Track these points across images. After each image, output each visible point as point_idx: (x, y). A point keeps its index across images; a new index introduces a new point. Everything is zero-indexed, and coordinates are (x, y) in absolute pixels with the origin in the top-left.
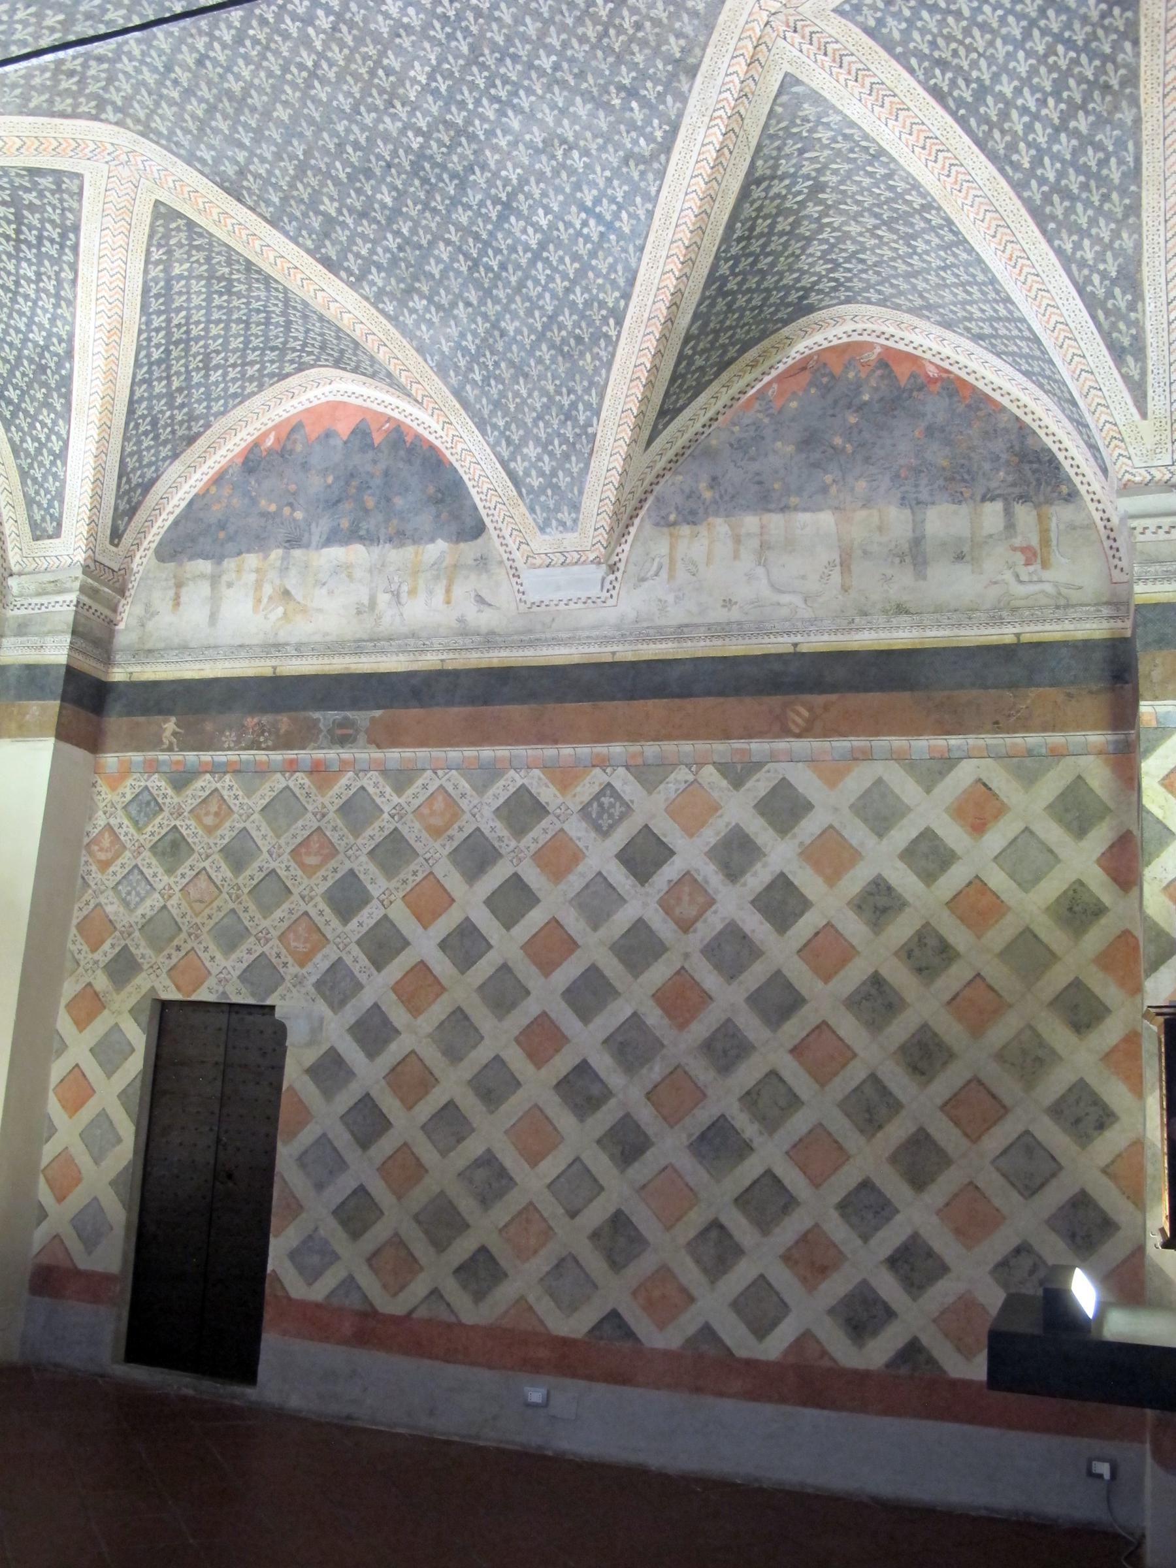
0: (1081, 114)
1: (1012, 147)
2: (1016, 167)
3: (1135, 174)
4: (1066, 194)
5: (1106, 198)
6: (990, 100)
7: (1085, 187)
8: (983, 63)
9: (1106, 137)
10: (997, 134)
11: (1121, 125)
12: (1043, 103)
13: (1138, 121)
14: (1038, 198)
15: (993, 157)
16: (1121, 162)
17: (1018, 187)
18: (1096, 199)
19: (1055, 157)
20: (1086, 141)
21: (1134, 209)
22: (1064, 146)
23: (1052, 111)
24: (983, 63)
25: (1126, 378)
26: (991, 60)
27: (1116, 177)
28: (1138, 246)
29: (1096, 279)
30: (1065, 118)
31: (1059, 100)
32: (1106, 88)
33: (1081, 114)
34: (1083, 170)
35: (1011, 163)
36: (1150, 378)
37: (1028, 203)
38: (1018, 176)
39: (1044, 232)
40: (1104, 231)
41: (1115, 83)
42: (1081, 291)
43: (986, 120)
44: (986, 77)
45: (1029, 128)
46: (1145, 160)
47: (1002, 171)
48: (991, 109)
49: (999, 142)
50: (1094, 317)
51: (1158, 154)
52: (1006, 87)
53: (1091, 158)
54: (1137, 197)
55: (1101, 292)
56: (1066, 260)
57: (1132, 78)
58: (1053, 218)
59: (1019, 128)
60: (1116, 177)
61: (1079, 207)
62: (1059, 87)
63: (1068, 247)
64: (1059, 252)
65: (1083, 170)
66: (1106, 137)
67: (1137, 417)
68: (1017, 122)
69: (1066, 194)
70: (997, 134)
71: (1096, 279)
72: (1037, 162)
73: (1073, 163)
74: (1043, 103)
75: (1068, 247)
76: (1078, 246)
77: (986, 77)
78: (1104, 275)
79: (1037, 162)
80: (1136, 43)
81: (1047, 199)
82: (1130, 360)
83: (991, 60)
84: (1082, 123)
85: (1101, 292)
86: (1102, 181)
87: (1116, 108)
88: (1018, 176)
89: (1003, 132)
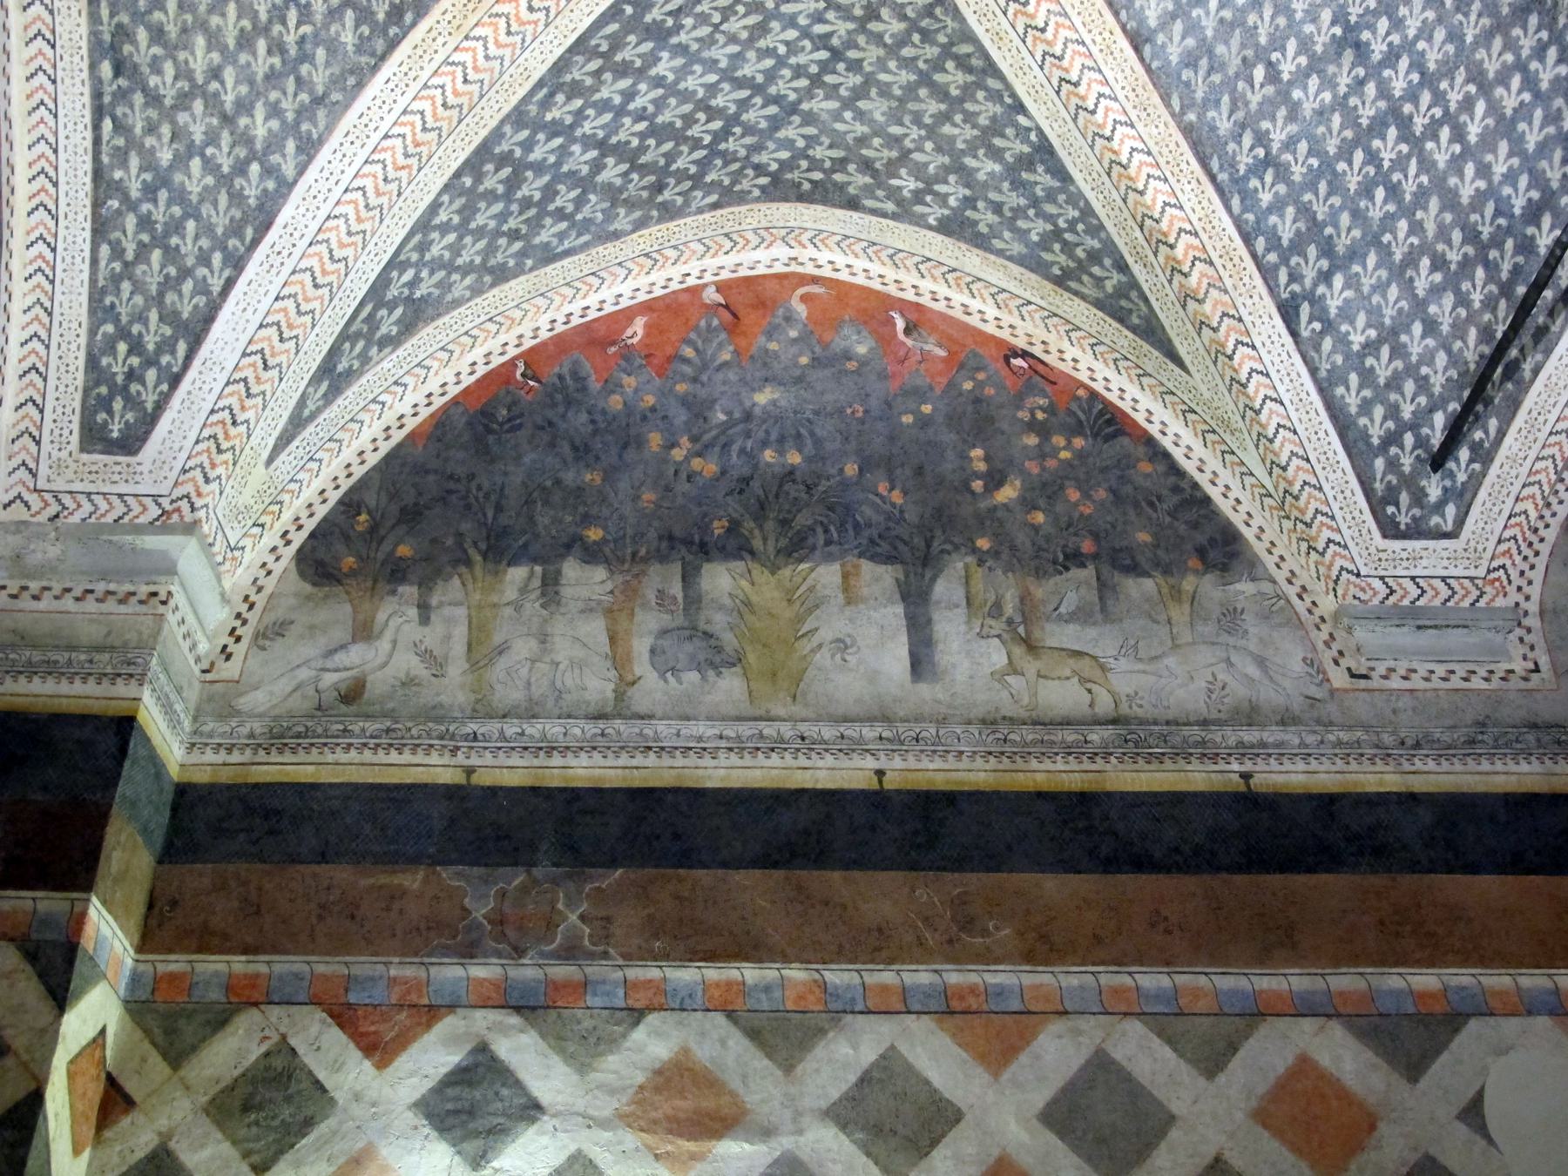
0: (624, 167)
1: (575, 90)
2: (546, 104)
3: (549, 256)
4: (513, 183)
5: (514, 235)
6: (648, 46)
7: (527, 203)
8: (705, 31)
9: (594, 206)
10: (594, 65)
11: (609, 216)
12: (640, 116)
13: (617, 235)
14: (505, 147)
15: (561, 66)
16: (561, 236)
17: (517, 117)
18: (512, 223)
19: (563, 152)
20: (585, 184)
21: (502, 275)
22: (580, 159)
23: (629, 131)
24: (705, 31)
25: (303, 399)
26: (708, 42)
27: (544, 237)
28: (457, 303)
29: (408, 275)
30: (621, 151)
31: (643, 136)
32: (659, 188)
33: (624, 167)
34: (549, 192)
35: (552, 95)
36: (311, 428)
37: (497, 135)
38: (533, 109)
39: (458, 175)
40: (471, 252)
41: (667, 195)
42: (389, 266)
43: (616, 43)
44: (683, 37)
45: (604, 106)
46: (566, 262)
47: (540, 84)
48: (634, 50)
49: (580, 72)
50: (362, 304)
51: (576, 274)
52: (665, 66)
53: (565, 198)
54: (519, 271)
55: (393, 292)
56: (424, 225)
57: (669, 212)
58: (479, 179)
59: (604, 93)
60: (544, 237)
61: (498, 207)
62: (659, 132)
63: (443, 216)
64: (434, 207)
65: (549, 192)
66: (594, 206)
67: (265, 455)
68: (611, 90)
69: (513, 183)
70: (594, 65)
71: (408, 275)
72: (555, 129)
73: (557, 179)
74: (640, 116)
75: (443, 216)
76: (445, 229)
77: (683, 37)
78: (414, 283)
79: (555, 129)
80: (715, 206)
81: (504, 160)
82: (324, 386)
83: (708, 42)
84: (612, 172)
85: (393, 292)
86: (536, 224)
87: (631, 205)
88: (533, 109)
89: (597, 74)
